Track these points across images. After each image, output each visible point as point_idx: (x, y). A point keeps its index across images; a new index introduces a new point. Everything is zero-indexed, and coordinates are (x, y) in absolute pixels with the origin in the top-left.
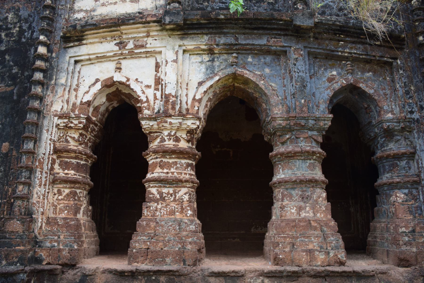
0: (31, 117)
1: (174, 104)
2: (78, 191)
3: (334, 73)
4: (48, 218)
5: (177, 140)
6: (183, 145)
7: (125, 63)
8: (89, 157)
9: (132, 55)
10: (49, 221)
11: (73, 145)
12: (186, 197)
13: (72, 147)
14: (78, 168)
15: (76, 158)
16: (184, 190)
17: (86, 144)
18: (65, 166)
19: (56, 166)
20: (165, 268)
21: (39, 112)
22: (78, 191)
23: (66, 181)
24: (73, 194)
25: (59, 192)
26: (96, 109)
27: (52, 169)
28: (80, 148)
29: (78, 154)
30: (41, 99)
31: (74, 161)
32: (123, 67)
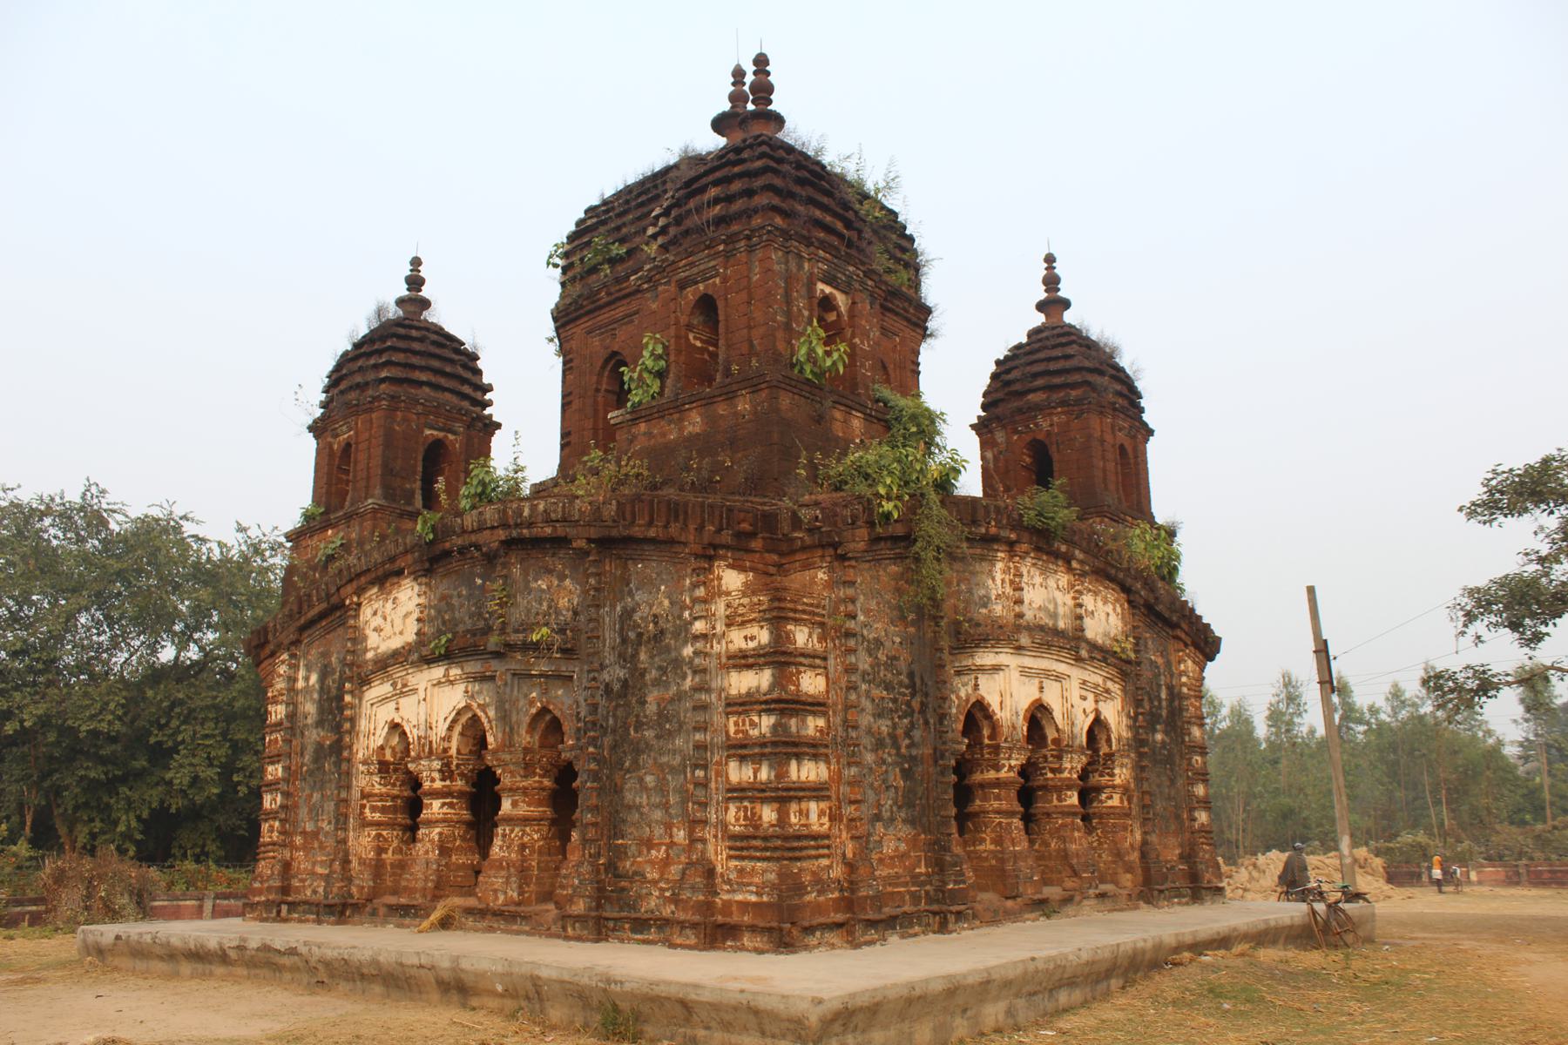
0: (344, 766)
1: (424, 745)
2: (384, 833)
3: (534, 694)
4: (360, 858)
5: (433, 780)
6: (438, 784)
7: (403, 701)
8: (394, 798)
9: (402, 693)
10: (362, 862)
11: (378, 789)
12: (436, 838)
13: (377, 791)
14: (383, 810)
15: (381, 800)
16: (437, 830)
17: (394, 785)
18: (373, 809)
19: (367, 810)
20: (415, 903)
21: (349, 760)
22: (384, 833)
23: (378, 824)
24: (379, 836)
25: (369, 835)
26: (393, 749)
27: (362, 813)
28: (384, 790)
29: (381, 797)
30: (350, 747)
31: (379, 804)
32: (400, 706)
